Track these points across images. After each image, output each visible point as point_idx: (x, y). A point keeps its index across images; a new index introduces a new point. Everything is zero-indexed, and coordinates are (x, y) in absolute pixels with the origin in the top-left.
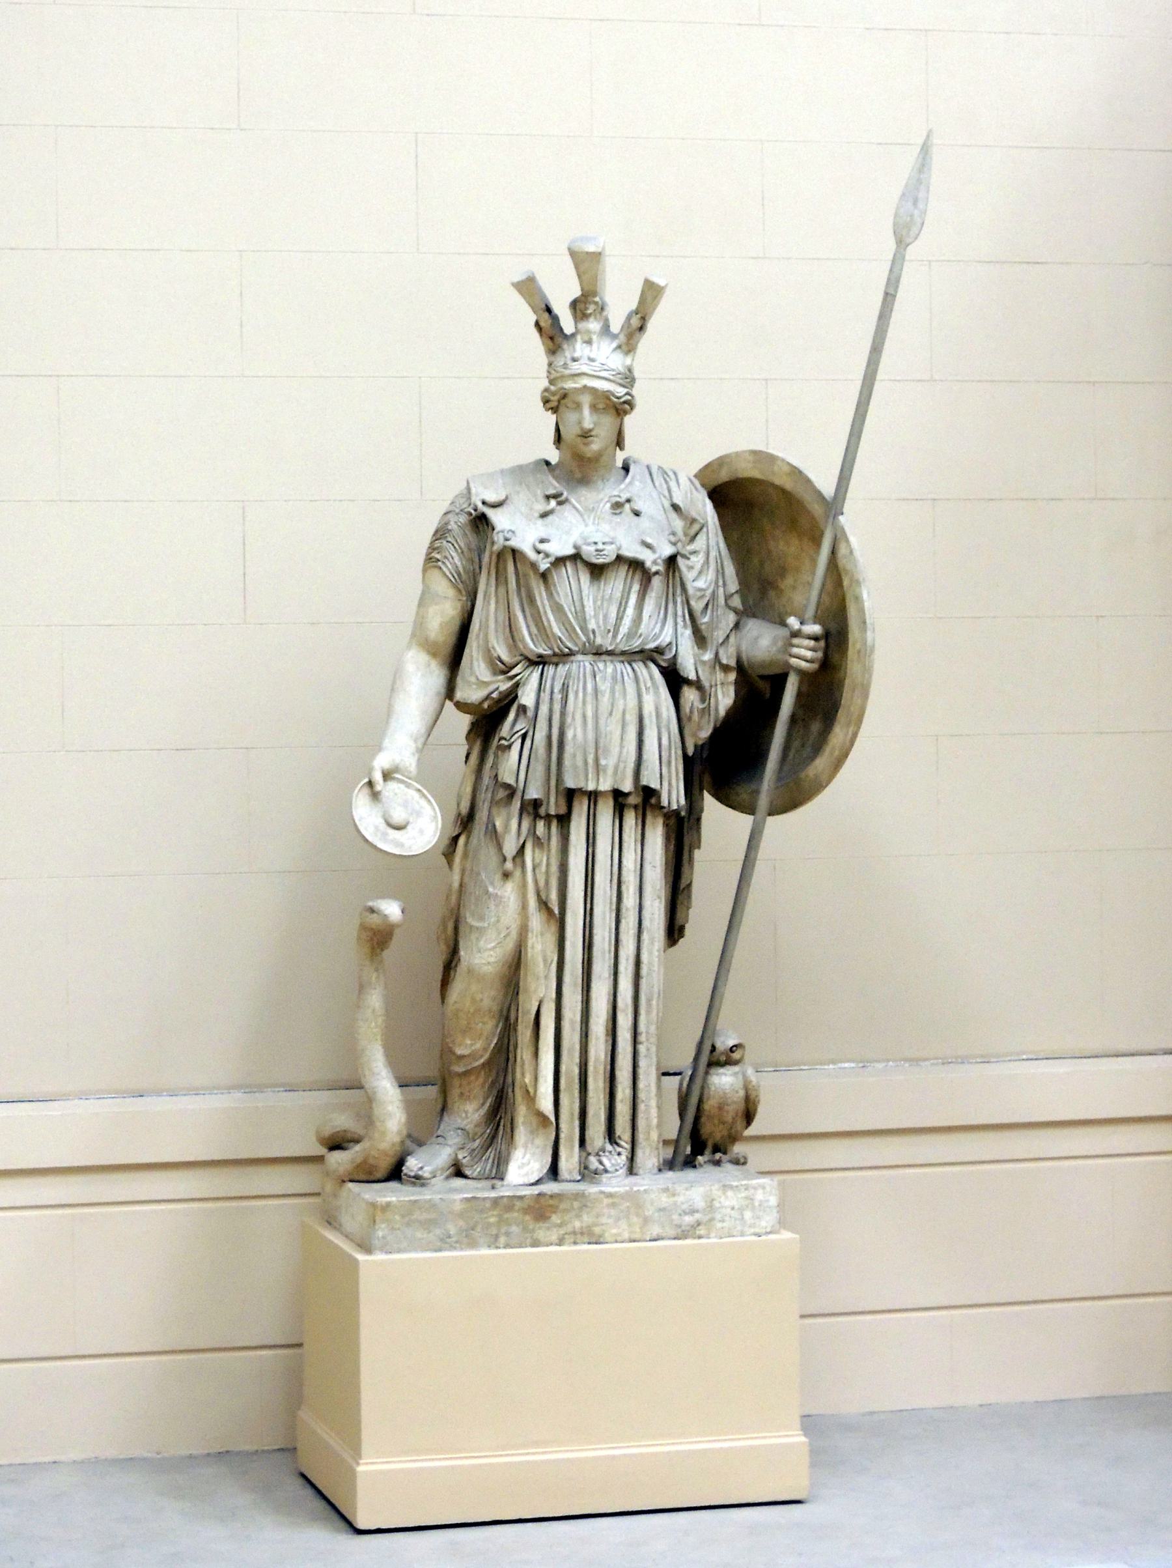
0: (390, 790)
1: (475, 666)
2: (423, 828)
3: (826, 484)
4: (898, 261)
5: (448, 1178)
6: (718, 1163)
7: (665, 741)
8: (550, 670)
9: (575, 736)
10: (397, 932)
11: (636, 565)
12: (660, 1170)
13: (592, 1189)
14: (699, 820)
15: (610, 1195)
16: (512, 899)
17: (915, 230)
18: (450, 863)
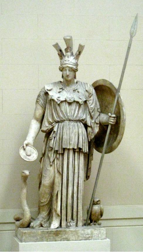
0: (28, 148)
2: (34, 156)
3: (116, 85)
4: (131, 41)
5: (39, 227)
6: (95, 225)
7: (84, 138)
8: (60, 124)
9: (65, 137)
10: (28, 177)
11: (78, 102)
12: (83, 226)
13: (68, 230)
14: (92, 155)
15: (71, 231)
16: (52, 170)
17: (134, 35)
18: (41, 163)
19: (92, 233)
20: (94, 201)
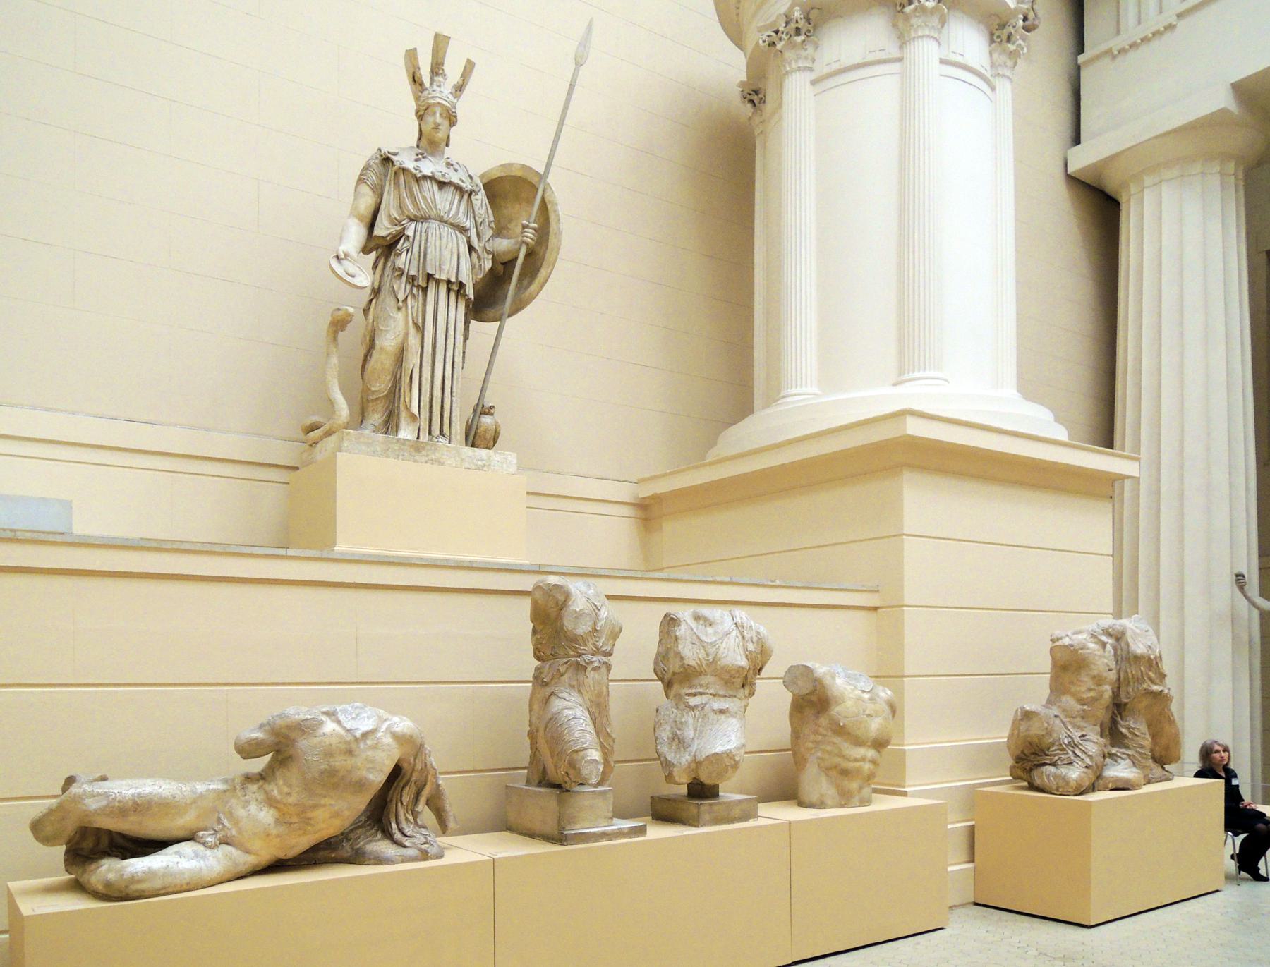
8: (419, 225)
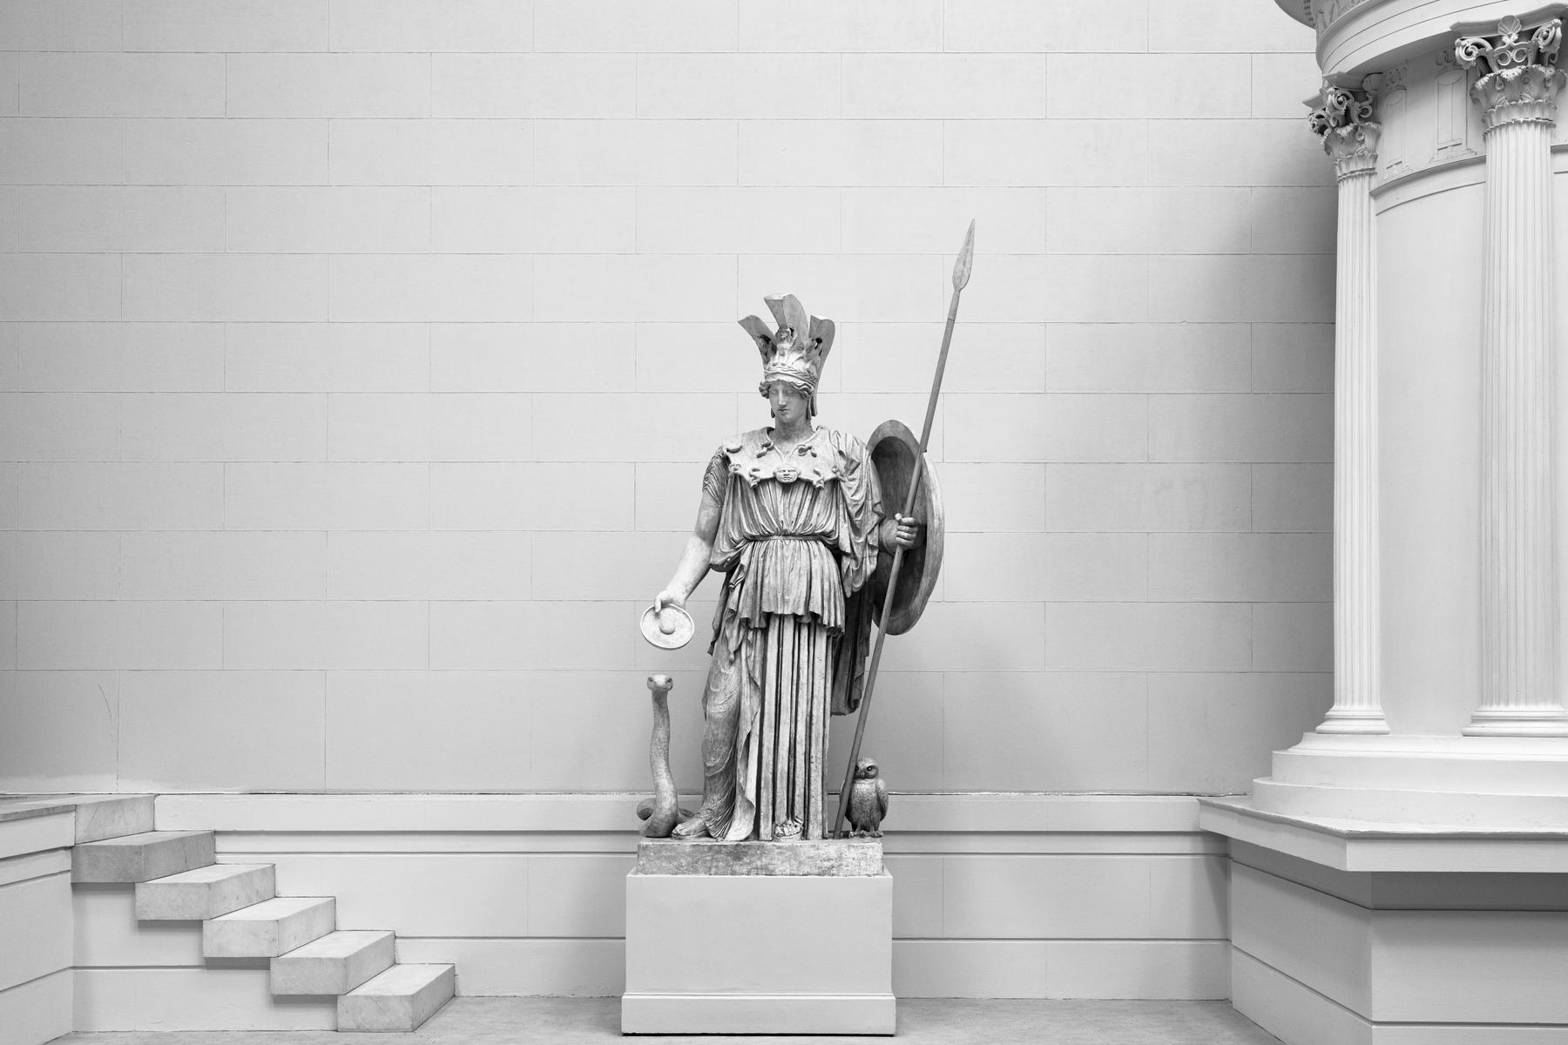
1: (723, 546)
6: (862, 836)
8: (758, 545)
11: (809, 483)
19: (840, 857)
20: (857, 768)
